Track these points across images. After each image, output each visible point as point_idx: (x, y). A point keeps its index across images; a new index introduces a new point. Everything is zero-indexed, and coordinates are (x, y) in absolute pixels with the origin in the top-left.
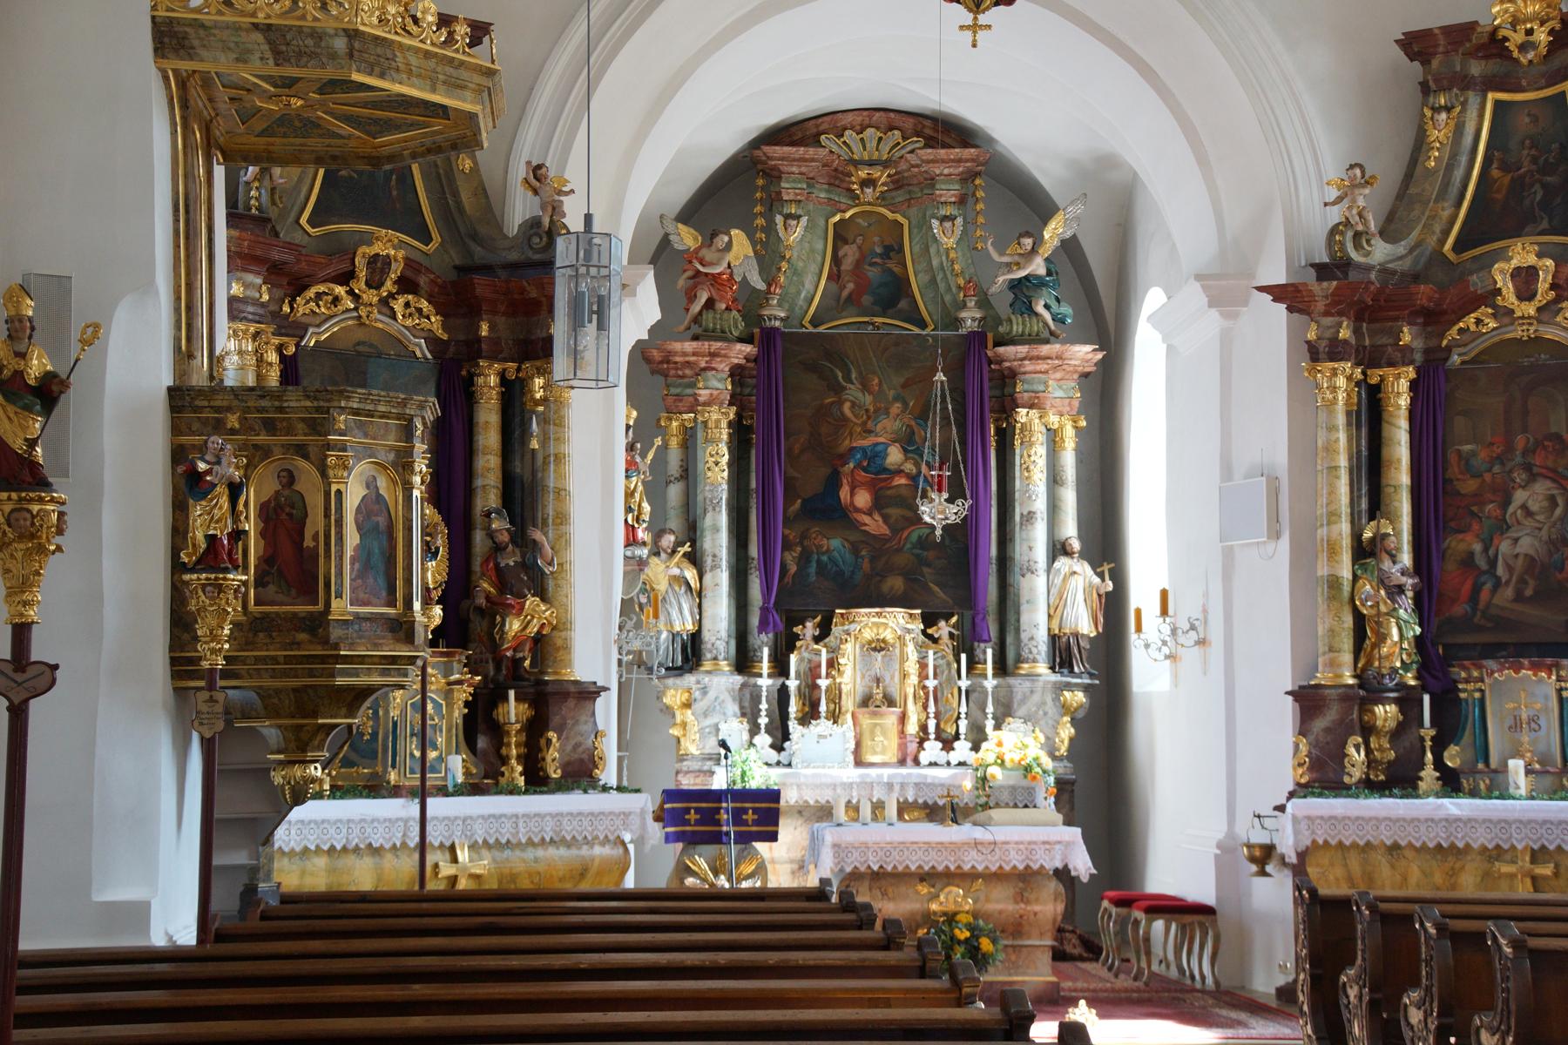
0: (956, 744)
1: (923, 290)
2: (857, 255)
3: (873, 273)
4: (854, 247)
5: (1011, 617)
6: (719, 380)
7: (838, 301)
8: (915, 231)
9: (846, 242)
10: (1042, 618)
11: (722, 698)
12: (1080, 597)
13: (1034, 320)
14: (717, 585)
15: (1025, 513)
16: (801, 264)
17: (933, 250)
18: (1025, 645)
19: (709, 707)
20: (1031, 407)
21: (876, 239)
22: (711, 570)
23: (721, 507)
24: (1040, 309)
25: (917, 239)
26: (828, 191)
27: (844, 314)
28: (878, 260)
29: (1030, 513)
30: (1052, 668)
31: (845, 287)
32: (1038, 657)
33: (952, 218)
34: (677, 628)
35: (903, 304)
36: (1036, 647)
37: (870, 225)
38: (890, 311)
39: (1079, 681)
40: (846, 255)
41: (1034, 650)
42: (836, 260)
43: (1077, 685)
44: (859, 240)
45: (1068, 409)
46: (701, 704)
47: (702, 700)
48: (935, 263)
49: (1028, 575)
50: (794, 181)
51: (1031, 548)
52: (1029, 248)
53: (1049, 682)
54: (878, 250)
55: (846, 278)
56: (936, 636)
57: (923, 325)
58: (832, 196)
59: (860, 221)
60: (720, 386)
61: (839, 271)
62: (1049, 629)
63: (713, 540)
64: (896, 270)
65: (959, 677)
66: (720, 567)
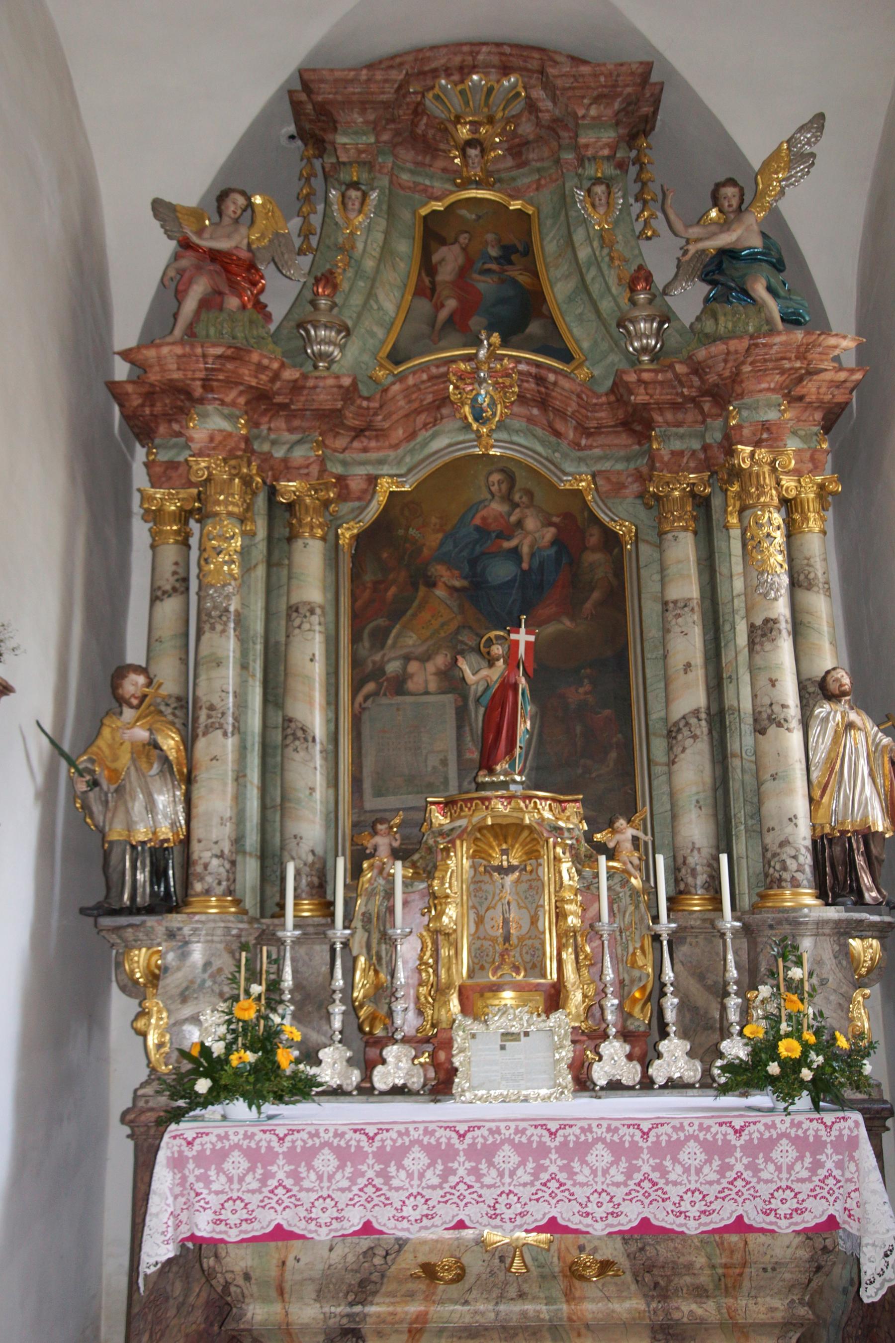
0: (663, 1046)
1: (564, 307)
2: (461, 260)
3: (485, 285)
4: (456, 248)
5: (739, 811)
6: (228, 417)
7: (433, 325)
8: (549, 222)
9: (443, 242)
10: (800, 805)
11: (217, 963)
12: (863, 767)
13: (752, 309)
14: (215, 758)
15: (758, 622)
16: (369, 264)
17: (579, 236)
18: (775, 855)
19: (192, 982)
20: (758, 444)
21: (490, 237)
22: (204, 734)
23: (225, 624)
24: (760, 290)
25: (551, 235)
26: (412, 172)
27: (442, 344)
28: (494, 266)
29: (767, 621)
30: (822, 894)
31: (443, 306)
32: (799, 876)
33: (607, 182)
34: (142, 833)
35: (534, 328)
36: (795, 857)
37: (479, 217)
38: (514, 339)
39: (876, 918)
40: (443, 260)
41: (792, 865)
42: (428, 267)
43: (873, 925)
44: (464, 239)
45: (810, 466)
46: (179, 975)
47: (179, 969)
48: (583, 253)
49: (772, 730)
50: (356, 133)
51: (773, 683)
52: (735, 202)
53: (827, 922)
54: (494, 252)
55: (445, 293)
56: (611, 845)
57: (566, 356)
58: (420, 180)
59: (464, 212)
60: (225, 425)
61: (433, 283)
62: (814, 827)
63: (209, 679)
64: (523, 279)
65: (656, 919)
66: (221, 726)
